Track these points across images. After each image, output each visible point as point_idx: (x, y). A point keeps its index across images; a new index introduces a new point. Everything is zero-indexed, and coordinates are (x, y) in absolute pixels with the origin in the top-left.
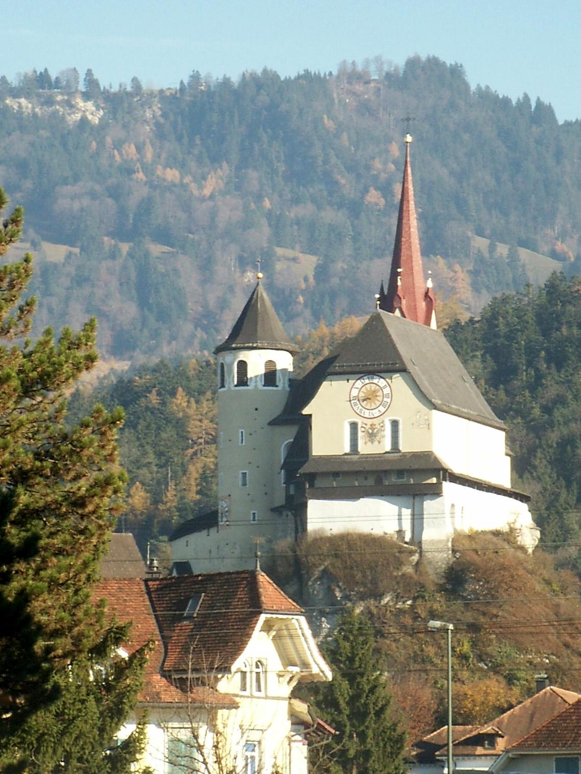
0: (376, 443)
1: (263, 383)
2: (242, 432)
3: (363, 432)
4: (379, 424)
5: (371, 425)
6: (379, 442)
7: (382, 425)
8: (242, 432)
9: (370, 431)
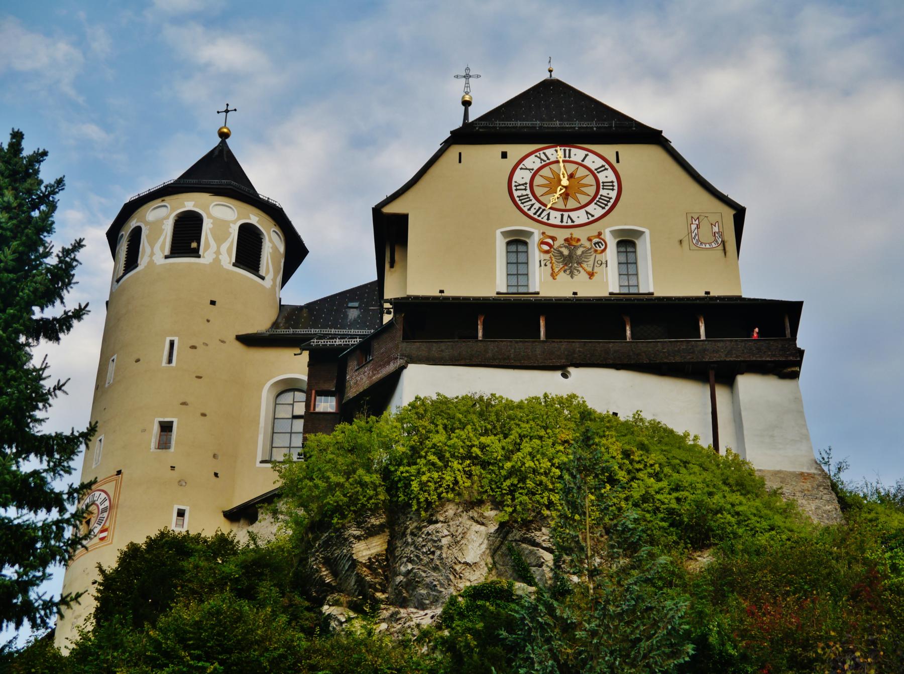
0: (582, 276)
1: (233, 260)
2: (172, 344)
3: (547, 252)
4: (590, 240)
5: (566, 240)
6: (591, 275)
8: (172, 344)
9: (566, 252)
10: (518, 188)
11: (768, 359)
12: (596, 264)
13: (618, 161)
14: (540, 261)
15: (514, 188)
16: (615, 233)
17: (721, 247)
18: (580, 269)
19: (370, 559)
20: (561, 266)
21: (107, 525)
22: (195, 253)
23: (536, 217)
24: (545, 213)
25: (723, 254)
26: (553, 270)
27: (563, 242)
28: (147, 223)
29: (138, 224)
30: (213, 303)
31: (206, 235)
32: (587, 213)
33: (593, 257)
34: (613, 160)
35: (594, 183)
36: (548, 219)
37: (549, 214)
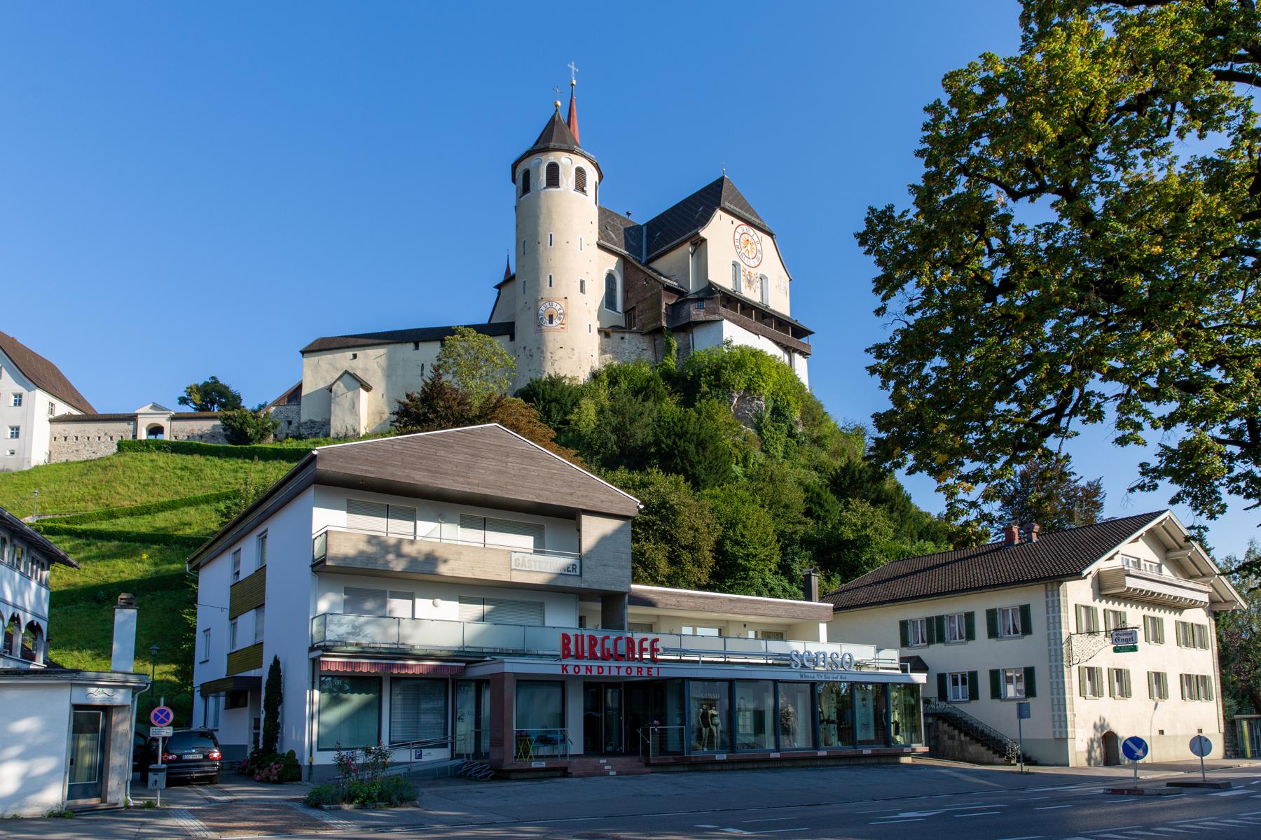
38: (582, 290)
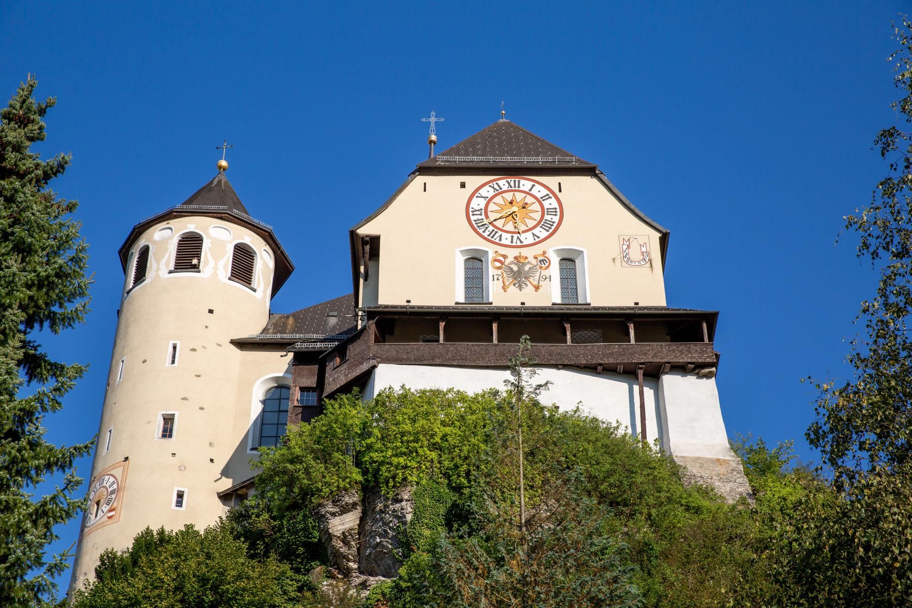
0: (530, 289)
1: (229, 275)
2: (175, 348)
3: (499, 268)
4: (536, 258)
5: (516, 258)
6: (537, 288)
7: (540, 258)
9: (515, 268)
10: (475, 213)
11: (689, 360)
12: (541, 279)
13: (560, 191)
14: (493, 276)
15: (471, 213)
16: (558, 251)
17: (648, 265)
18: (528, 283)
19: (343, 533)
20: (511, 280)
21: (115, 505)
22: (195, 268)
23: (490, 238)
24: (497, 235)
25: (649, 269)
26: (504, 283)
27: (513, 260)
28: (155, 242)
29: (146, 243)
30: (211, 311)
31: (206, 253)
32: (534, 235)
33: (538, 273)
34: (556, 190)
35: (540, 209)
36: (500, 240)
37: (501, 236)
38: (167, 433)
